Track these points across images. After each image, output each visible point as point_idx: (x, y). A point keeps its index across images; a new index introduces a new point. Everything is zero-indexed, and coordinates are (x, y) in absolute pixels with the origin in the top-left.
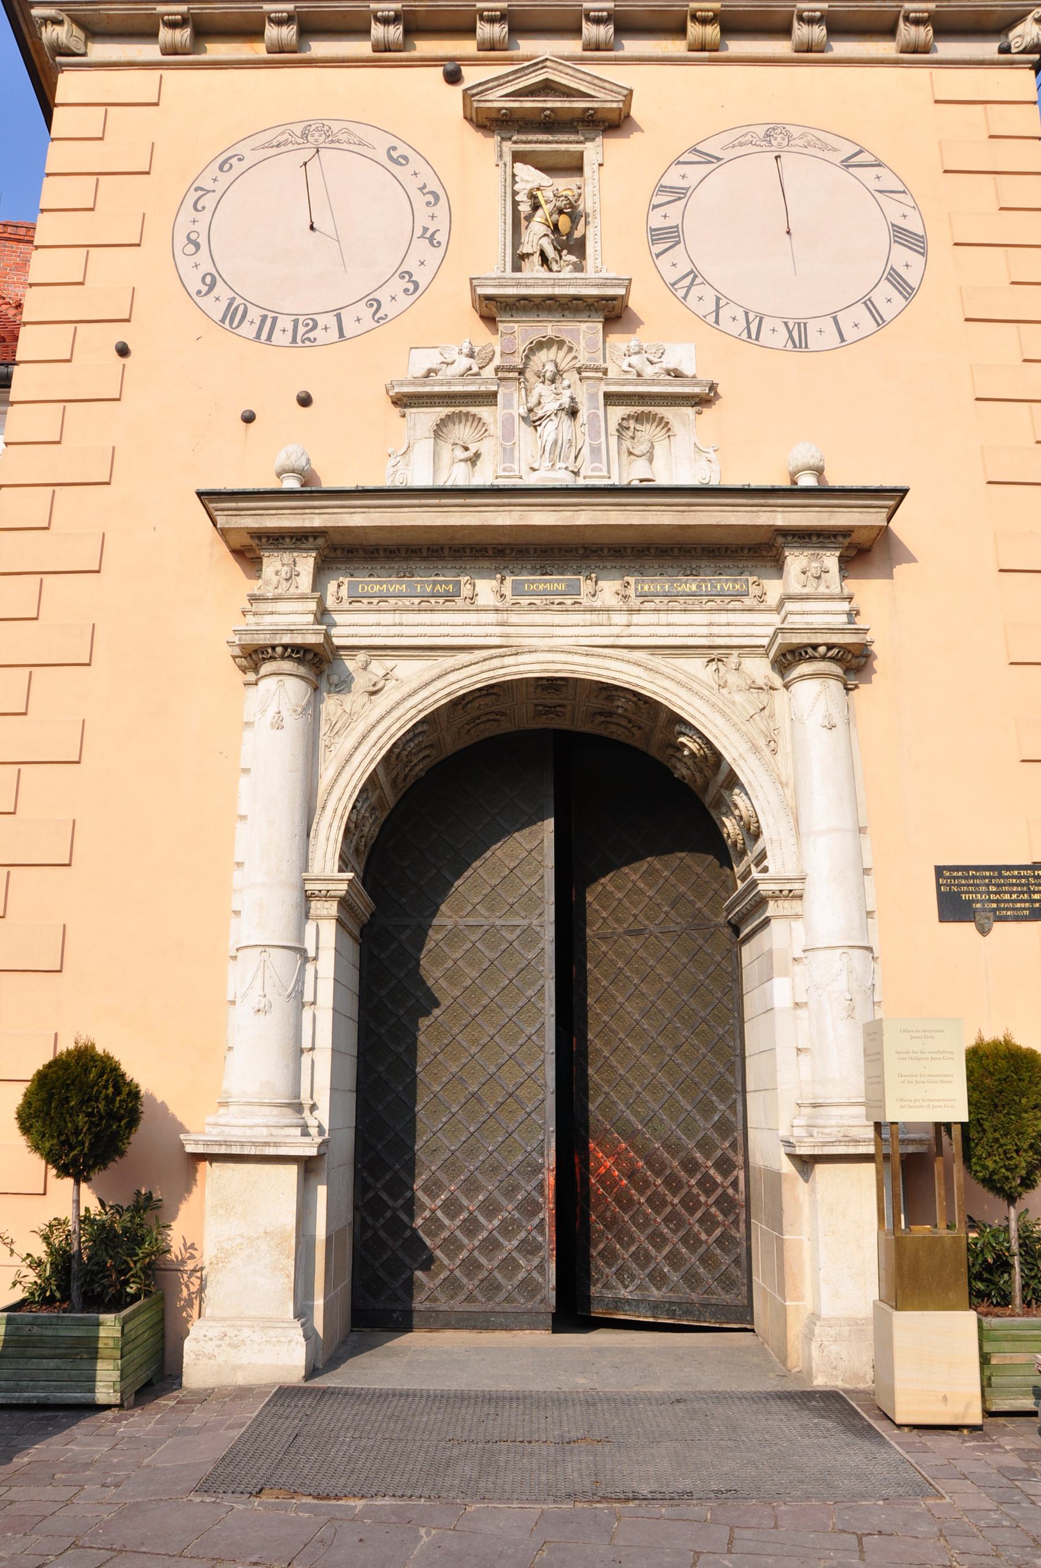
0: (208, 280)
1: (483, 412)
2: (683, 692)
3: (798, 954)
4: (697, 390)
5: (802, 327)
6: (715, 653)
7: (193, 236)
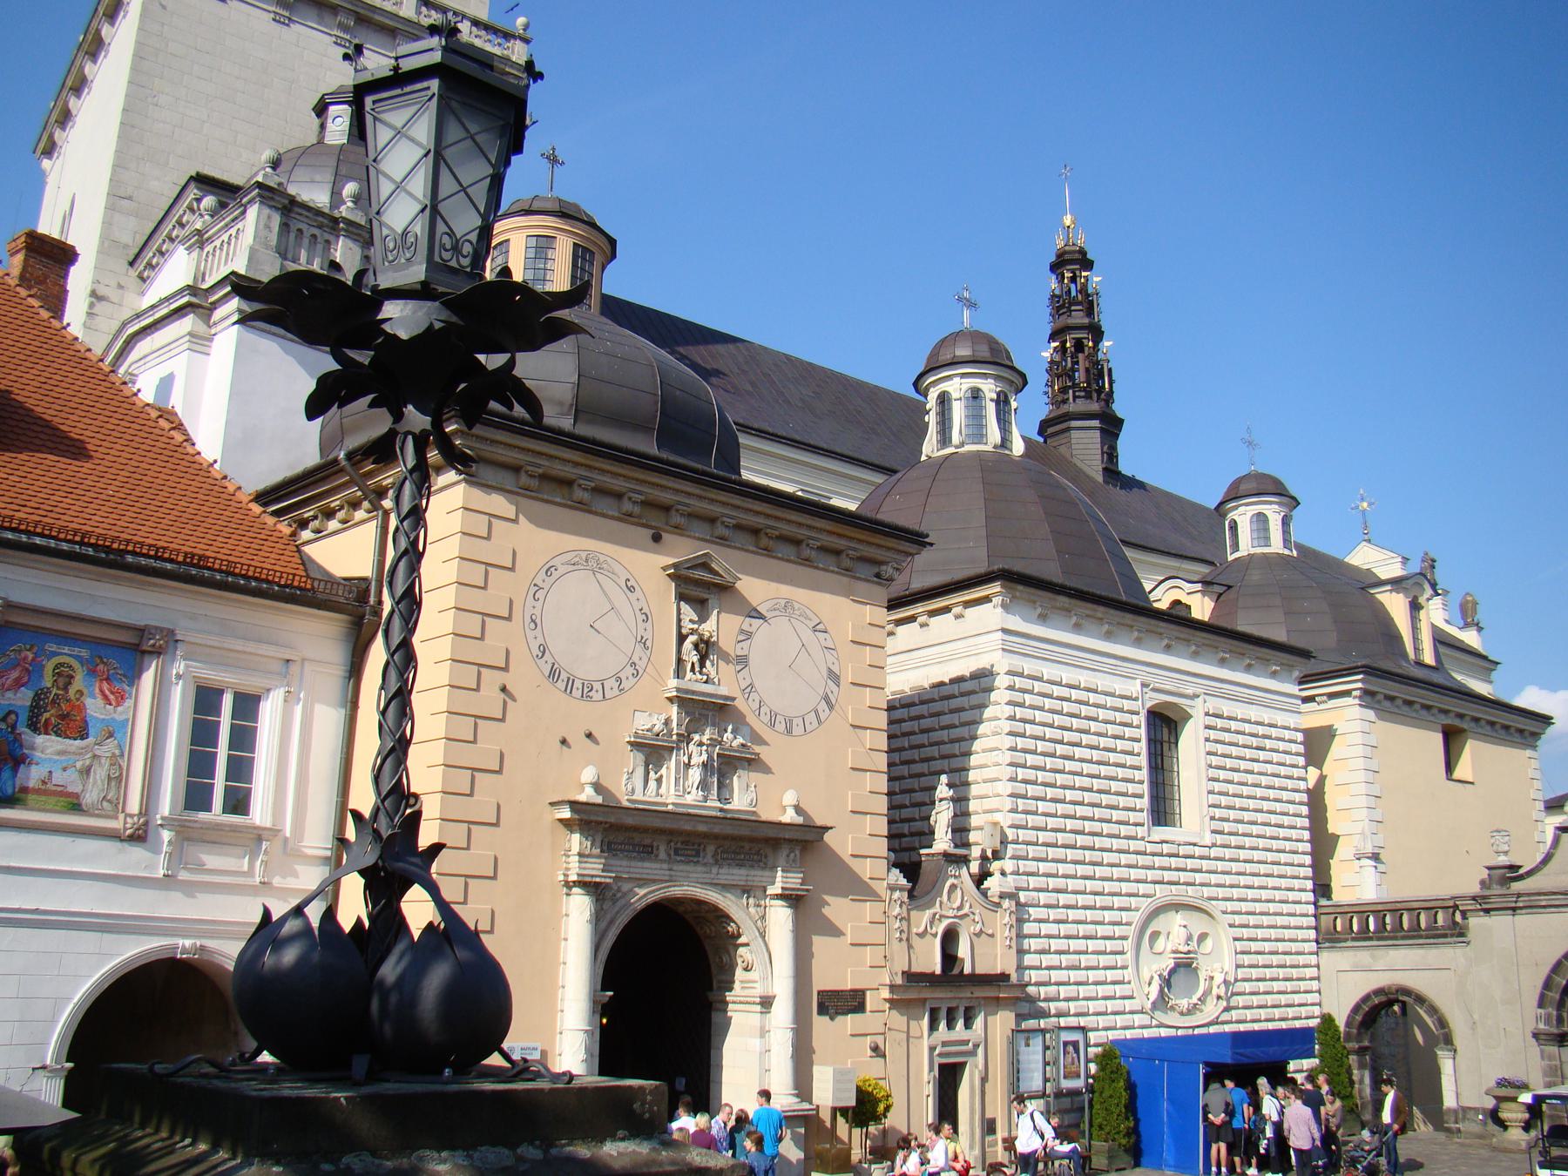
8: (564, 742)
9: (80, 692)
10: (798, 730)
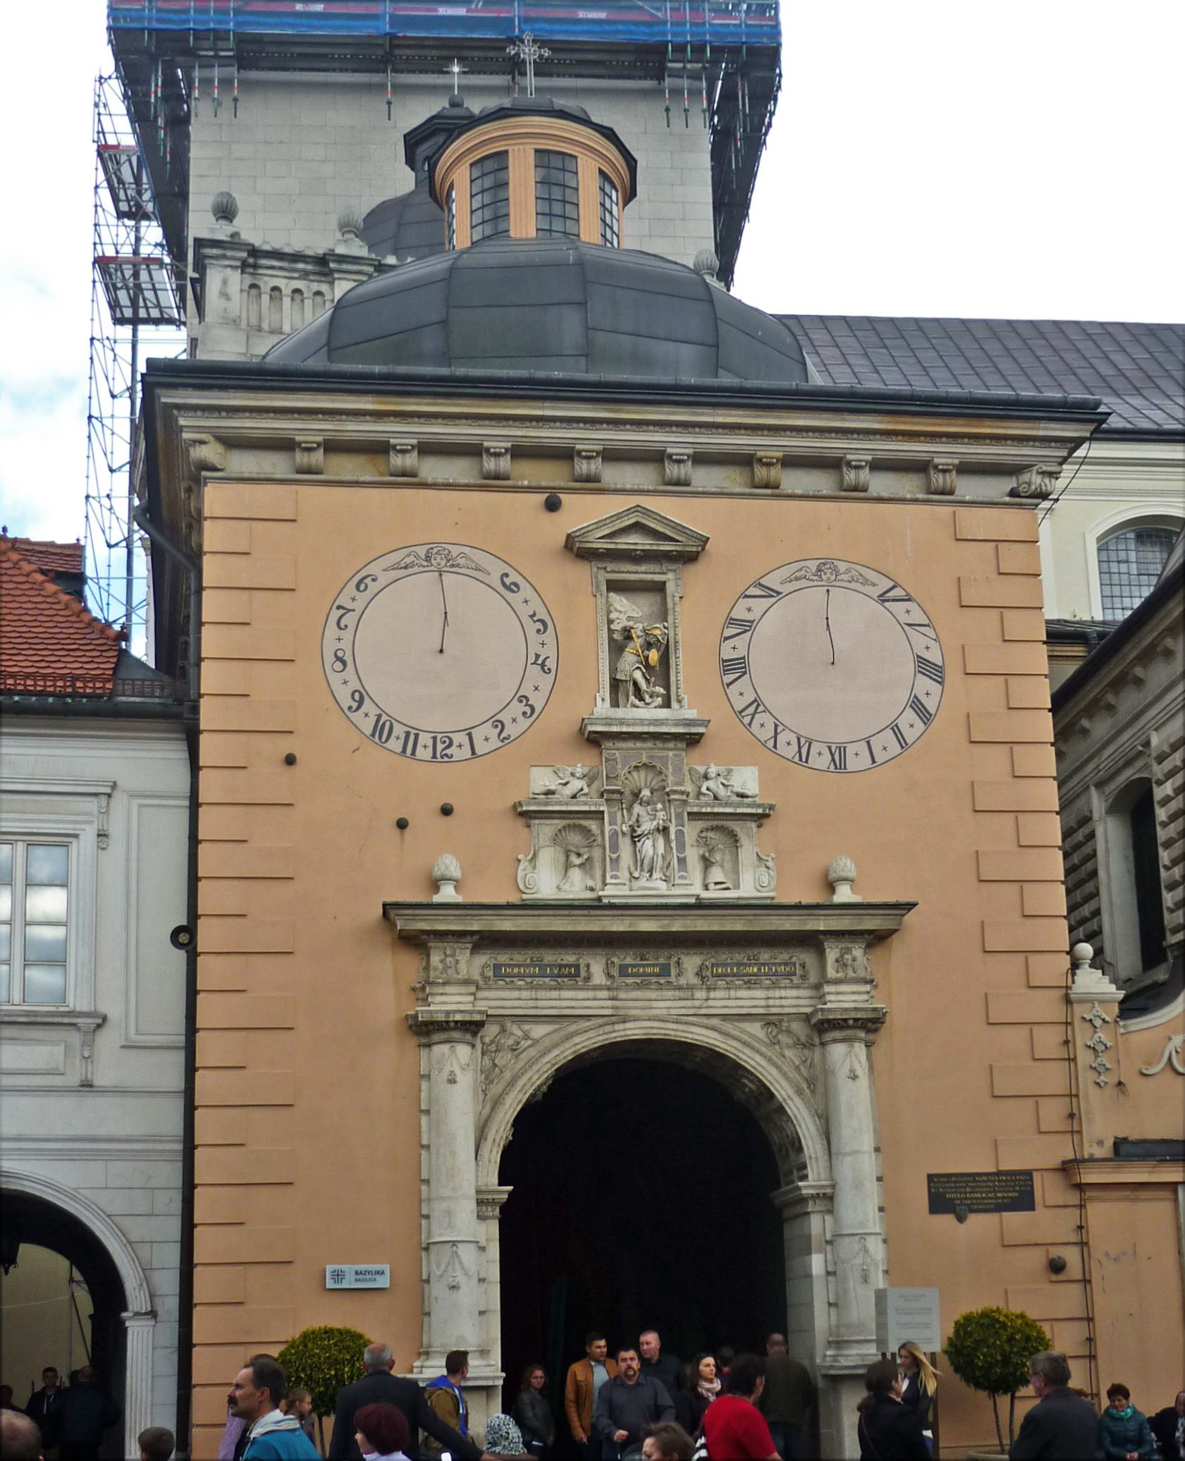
0: (357, 696)
1: (593, 825)
2: (746, 1050)
3: (828, 1238)
4: (760, 811)
5: (842, 749)
6: (770, 1021)
7: (340, 654)
8: (402, 825)
10: (857, 760)
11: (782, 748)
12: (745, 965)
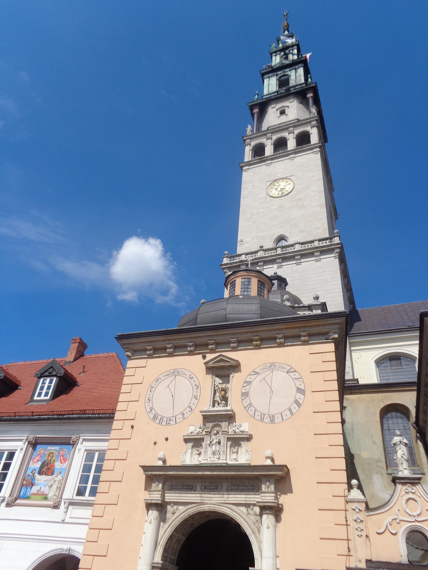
2: (238, 516)
4: (247, 436)
5: (274, 417)
6: (247, 505)
8: (155, 443)
9: (54, 461)
11: (256, 417)
12: (240, 486)
